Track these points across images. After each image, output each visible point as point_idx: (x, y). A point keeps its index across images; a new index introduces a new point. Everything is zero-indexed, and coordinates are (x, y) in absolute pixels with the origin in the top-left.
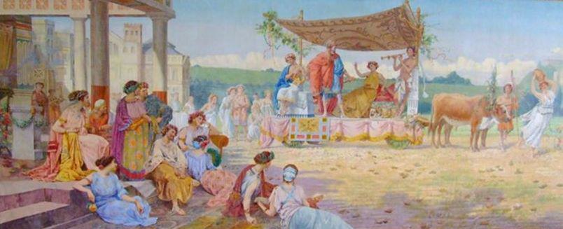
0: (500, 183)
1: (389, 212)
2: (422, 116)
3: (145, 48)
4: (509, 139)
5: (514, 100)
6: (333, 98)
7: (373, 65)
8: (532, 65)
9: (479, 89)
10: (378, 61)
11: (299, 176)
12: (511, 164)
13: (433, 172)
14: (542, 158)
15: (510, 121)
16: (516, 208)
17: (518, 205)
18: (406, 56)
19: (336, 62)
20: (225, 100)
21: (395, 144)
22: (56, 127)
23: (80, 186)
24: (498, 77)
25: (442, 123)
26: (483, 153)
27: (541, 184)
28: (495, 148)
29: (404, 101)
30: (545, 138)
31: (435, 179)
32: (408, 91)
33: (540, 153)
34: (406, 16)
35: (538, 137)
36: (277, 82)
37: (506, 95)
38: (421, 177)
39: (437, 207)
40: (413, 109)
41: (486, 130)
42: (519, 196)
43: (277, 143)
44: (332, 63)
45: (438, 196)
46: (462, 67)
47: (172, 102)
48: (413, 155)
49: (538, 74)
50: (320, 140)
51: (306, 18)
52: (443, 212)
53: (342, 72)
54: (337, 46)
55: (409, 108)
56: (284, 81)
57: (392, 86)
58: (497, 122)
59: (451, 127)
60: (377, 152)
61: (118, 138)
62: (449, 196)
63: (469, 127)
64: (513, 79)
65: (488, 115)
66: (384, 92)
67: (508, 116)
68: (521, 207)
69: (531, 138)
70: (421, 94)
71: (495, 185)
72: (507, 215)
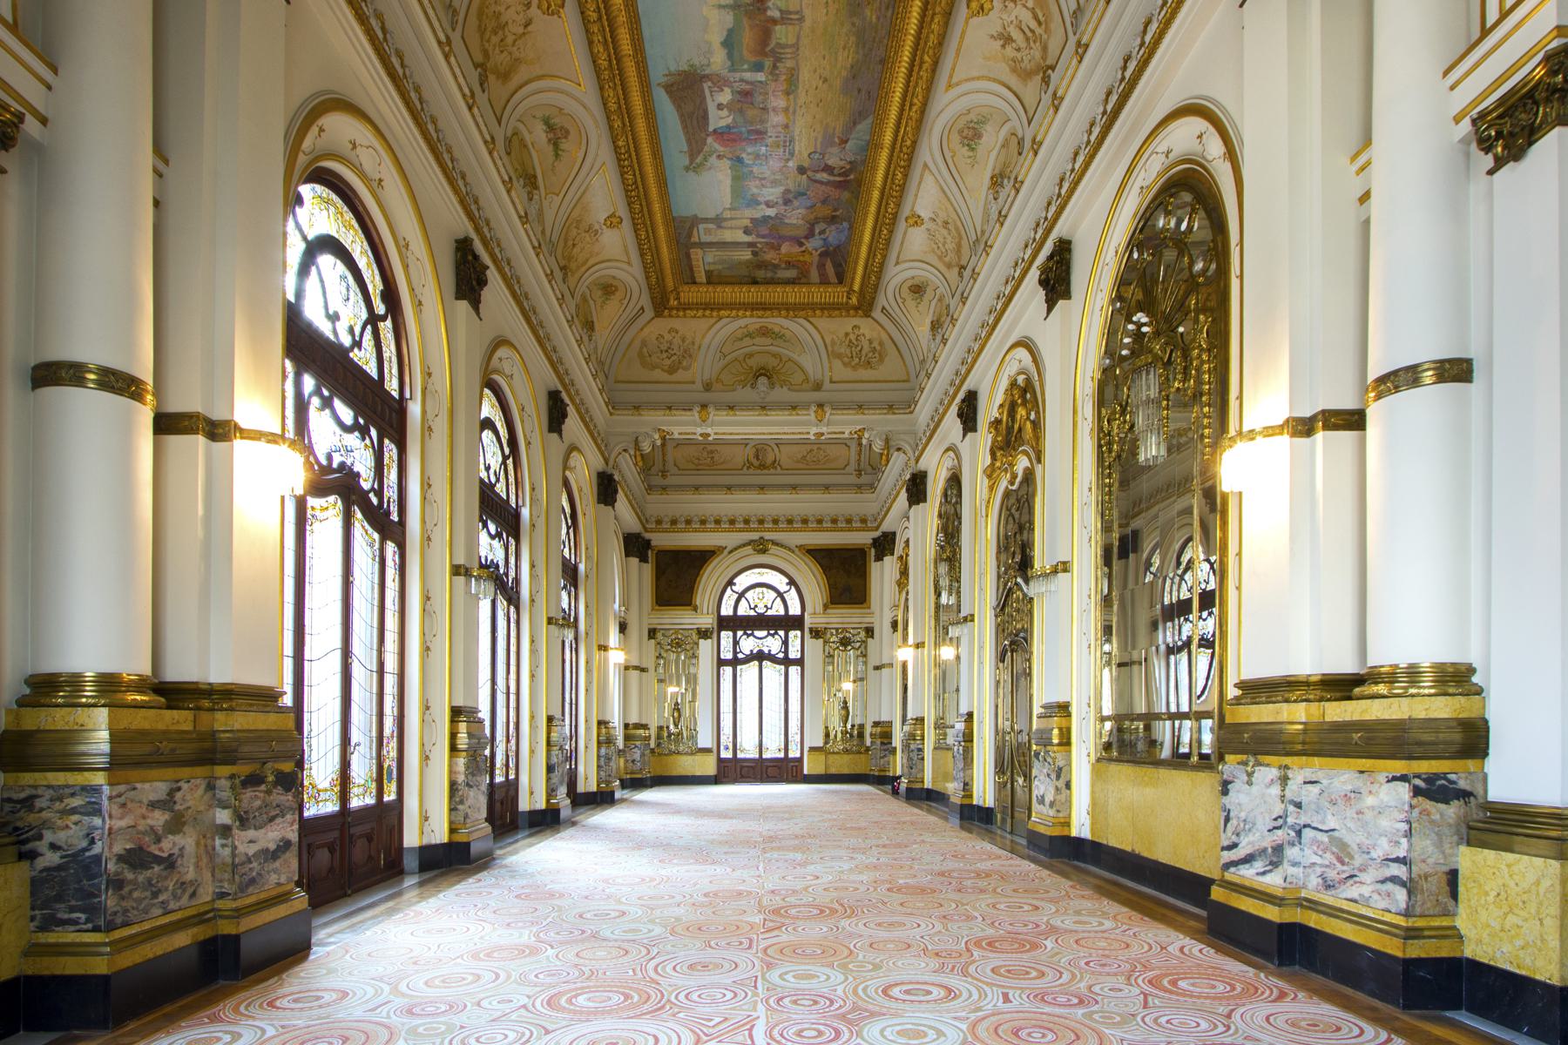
3: (720, 227)
6: (749, 132)
7: (720, 107)
9: (737, 20)
20: (755, 191)
23: (816, 254)
25: (773, 51)
26: (807, 12)
29: (751, 83)
32: (742, 80)
40: (760, 76)
43: (791, 164)
46: (716, 37)
47: (758, 215)
48: (805, 75)
51: (685, 148)
53: (728, 127)
56: (739, 160)
61: (783, 239)
63: (778, 28)
65: (765, 10)
66: (745, 96)
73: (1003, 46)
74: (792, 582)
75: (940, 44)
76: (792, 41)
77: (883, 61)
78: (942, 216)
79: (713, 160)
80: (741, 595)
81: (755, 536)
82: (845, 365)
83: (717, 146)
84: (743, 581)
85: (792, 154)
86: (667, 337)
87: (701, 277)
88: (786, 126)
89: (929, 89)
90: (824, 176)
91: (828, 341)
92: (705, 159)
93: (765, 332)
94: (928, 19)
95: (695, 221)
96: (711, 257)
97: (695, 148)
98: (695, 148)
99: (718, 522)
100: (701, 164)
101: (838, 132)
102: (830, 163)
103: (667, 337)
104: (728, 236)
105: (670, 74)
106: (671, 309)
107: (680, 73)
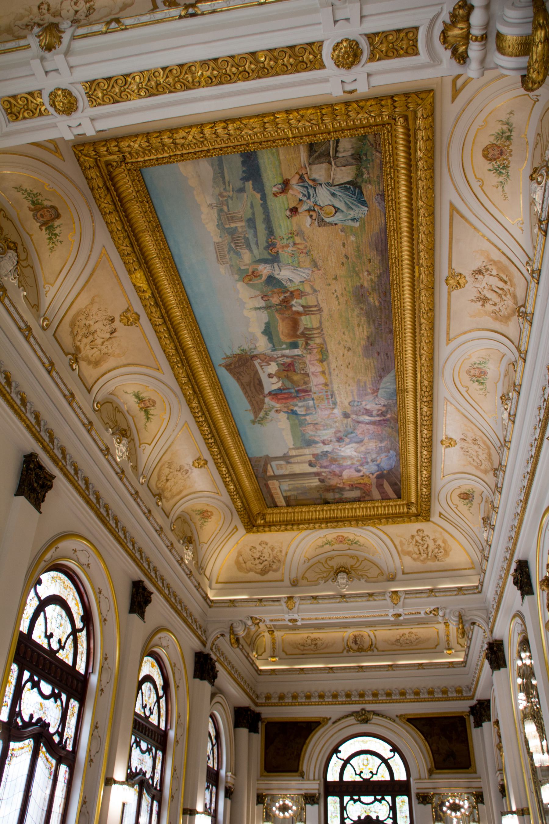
0: (347, 290)
1: (378, 354)
2: (300, 346)
3: (288, 463)
4: (308, 289)
5: (274, 293)
6: (298, 391)
8: (240, 286)
10: (266, 374)
11: (356, 399)
12: (329, 285)
13: (344, 333)
14: (320, 264)
15: (292, 292)
16: (369, 274)
17: (366, 274)
18: (259, 361)
19: (273, 393)
20: (311, 433)
21: (325, 357)
22: (341, 486)
24: (258, 306)
25: (303, 334)
26: (323, 305)
27: (344, 260)
28: (317, 298)
29: (292, 357)
30: (302, 264)
31: (349, 331)
32: (283, 356)
33: (315, 264)
34: (230, 365)
35: (302, 270)
36: (294, 416)
37: (271, 299)
38: (349, 340)
39: (373, 327)
40: (296, 352)
41: (303, 306)
42: (357, 274)
43: (336, 411)
44: (274, 395)
45: (363, 327)
48: (331, 346)
49: (247, 280)
50: (329, 393)
51: (249, 407)
52: (376, 322)
53: (279, 389)
54: (263, 393)
55: (297, 354)
56: (294, 413)
57: (283, 364)
58: (295, 300)
59: (306, 329)
60: (333, 366)
62: (362, 321)
63: (303, 318)
64: (256, 296)
65: (291, 307)
66: (288, 369)
67: (288, 294)
68: (368, 271)
69: (304, 275)
70: (284, 349)
71: (350, 292)
72: (376, 280)
73: (483, 305)
74: (395, 749)
75: (432, 310)
76: (316, 325)
77: (391, 331)
78: (470, 436)
79: (272, 414)
80: (347, 762)
81: (357, 708)
82: (414, 559)
83: (273, 403)
84: (347, 749)
85: (335, 404)
86: (259, 548)
87: (281, 502)
88: (326, 385)
89: (432, 343)
90: (367, 418)
91: (397, 543)
92: (266, 414)
93: (341, 540)
94: (417, 296)
95: (268, 460)
96: (286, 485)
97: (257, 406)
98: (257, 406)
99: (321, 696)
100: (263, 419)
101: (369, 385)
102: (368, 407)
103: (259, 548)
104: (298, 469)
105: (228, 357)
106: (259, 526)
107: (235, 356)
